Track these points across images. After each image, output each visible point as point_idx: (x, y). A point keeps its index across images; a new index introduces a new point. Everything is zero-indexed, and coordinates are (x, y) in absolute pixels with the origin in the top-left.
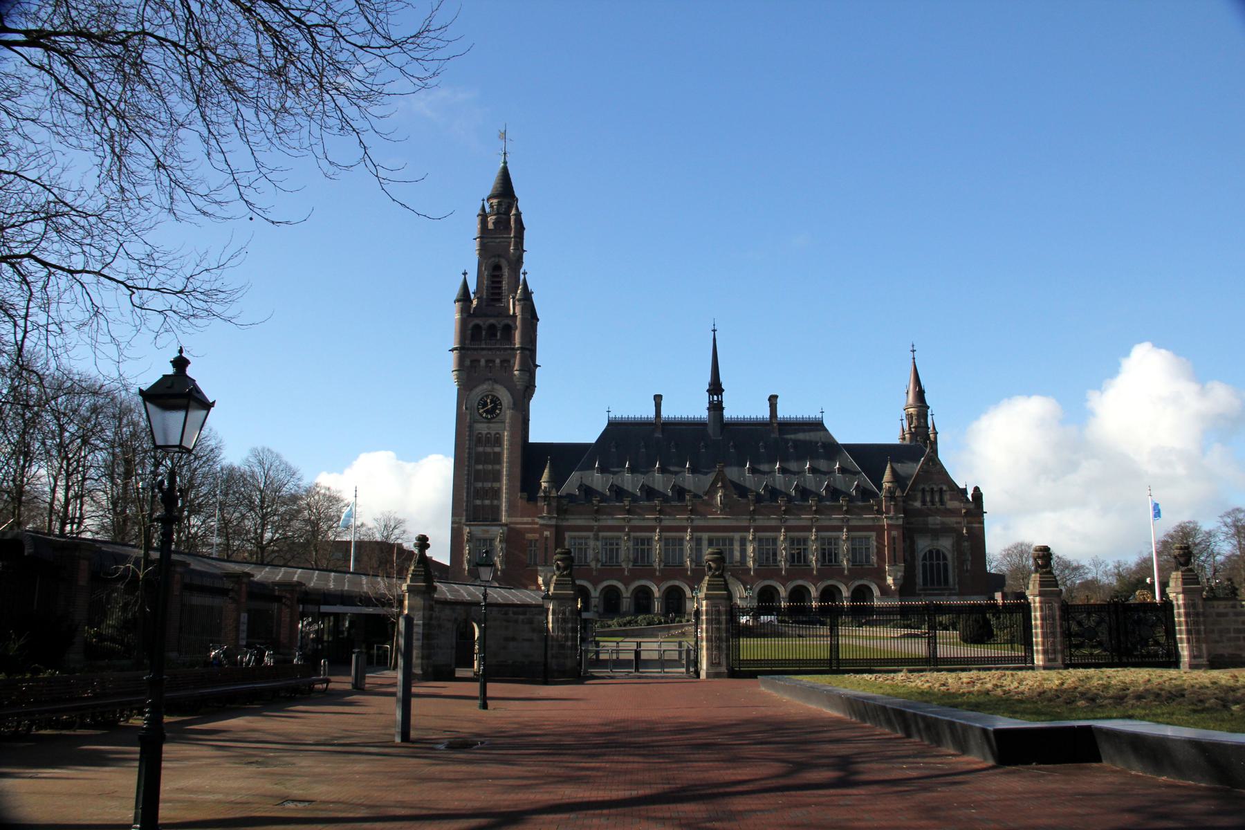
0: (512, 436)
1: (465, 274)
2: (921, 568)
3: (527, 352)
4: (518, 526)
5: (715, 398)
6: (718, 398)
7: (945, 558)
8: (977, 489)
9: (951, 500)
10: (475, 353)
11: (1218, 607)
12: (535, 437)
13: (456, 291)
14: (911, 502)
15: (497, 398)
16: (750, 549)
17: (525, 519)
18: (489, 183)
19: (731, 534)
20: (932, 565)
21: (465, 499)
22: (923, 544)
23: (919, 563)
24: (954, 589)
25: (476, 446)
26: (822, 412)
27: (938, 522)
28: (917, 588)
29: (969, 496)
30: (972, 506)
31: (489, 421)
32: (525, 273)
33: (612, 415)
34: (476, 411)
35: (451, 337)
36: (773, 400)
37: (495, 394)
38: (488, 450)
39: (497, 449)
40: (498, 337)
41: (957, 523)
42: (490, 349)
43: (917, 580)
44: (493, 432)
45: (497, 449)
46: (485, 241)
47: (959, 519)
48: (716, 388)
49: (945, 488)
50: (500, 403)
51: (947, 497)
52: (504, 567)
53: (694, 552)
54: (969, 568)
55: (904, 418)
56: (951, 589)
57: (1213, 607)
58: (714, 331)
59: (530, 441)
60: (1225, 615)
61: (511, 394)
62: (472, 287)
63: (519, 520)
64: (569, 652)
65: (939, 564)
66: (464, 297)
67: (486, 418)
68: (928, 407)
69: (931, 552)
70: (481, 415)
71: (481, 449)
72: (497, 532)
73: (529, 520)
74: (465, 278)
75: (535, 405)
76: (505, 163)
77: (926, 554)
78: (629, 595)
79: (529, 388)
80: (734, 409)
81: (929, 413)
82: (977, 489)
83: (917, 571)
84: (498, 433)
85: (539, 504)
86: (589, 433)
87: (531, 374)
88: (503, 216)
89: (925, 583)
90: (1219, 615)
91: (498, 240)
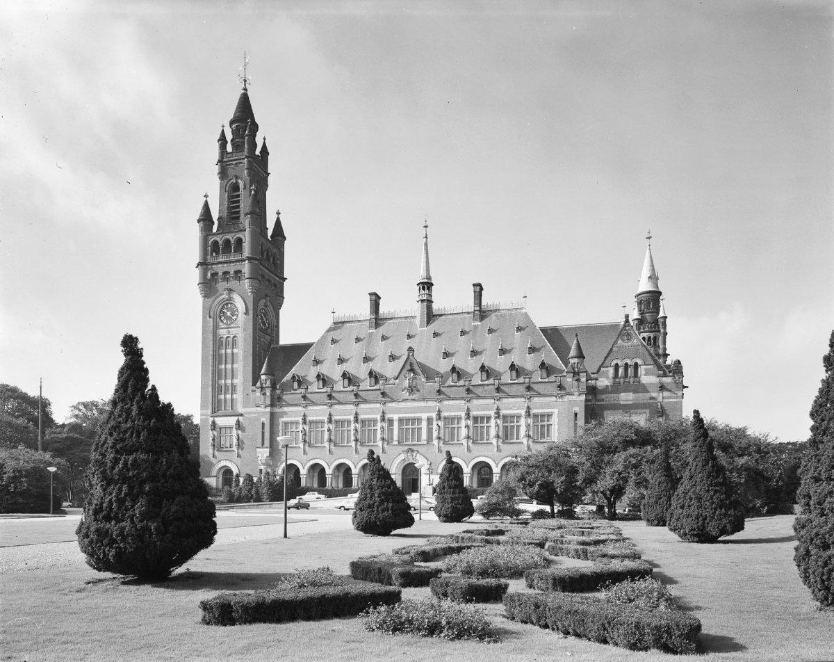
0: (245, 340)
1: (206, 196)
9: (646, 374)
13: (198, 212)
16: (435, 427)
18: (230, 111)
27: (631, 398)
39: (235, 351)
42: (227, 263)
49: (639, 362)
51: (642, 370)
53: (386, 432)
66: (206, 217)
70: (222, 321)
72: (232, 421)
76: (245, 89)
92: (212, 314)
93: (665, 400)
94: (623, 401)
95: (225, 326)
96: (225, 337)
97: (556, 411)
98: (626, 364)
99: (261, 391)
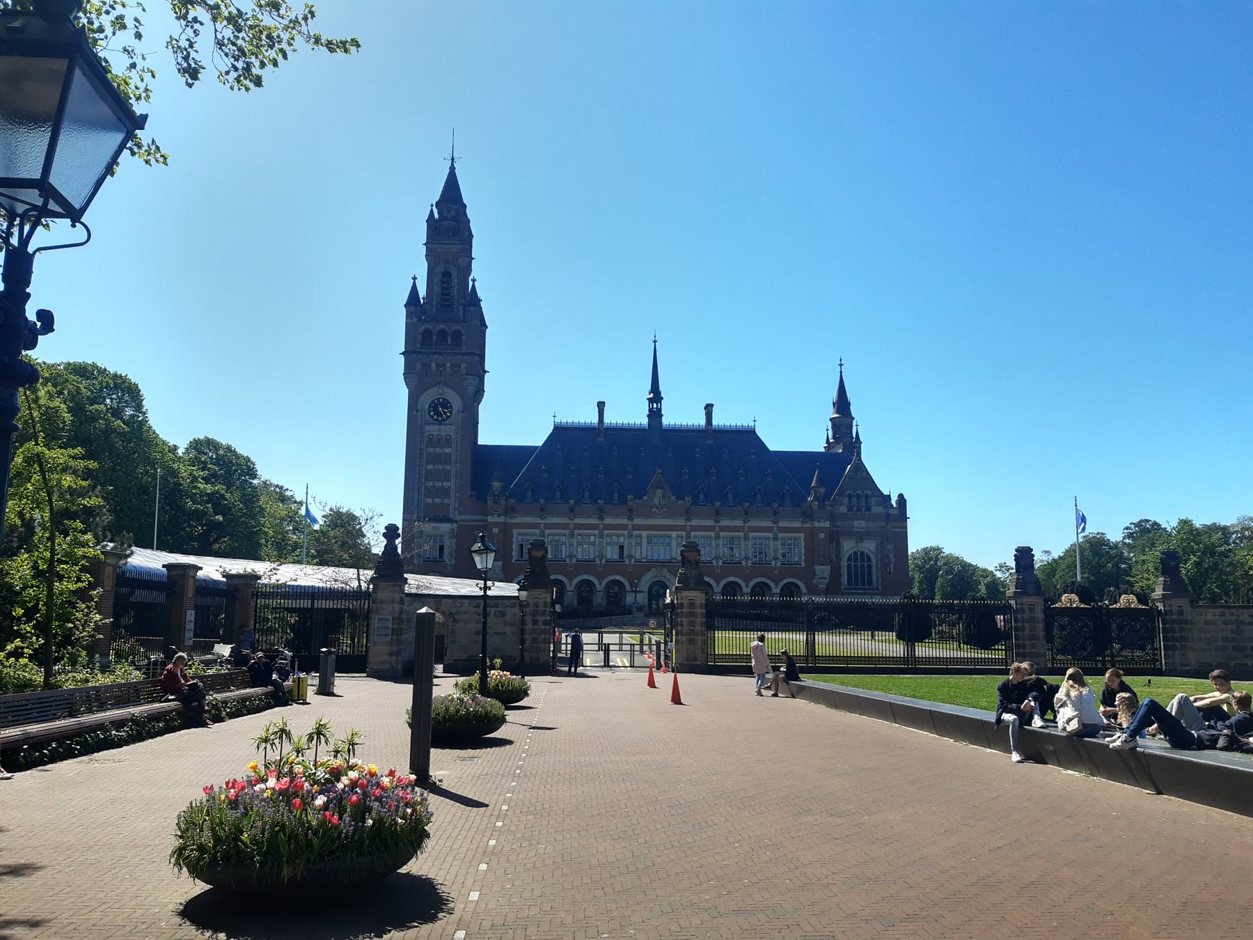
1: (415, 278)
2: (846, 568)
3: (476, 357)
4: (467, 523)
5: (655, 405)
6: (657, 406)
7: (869, 559)
8: (901, 496)
9: (876, 505)
10: (426, 356)
11: (1206, 615)
12: (486, 437)
14: (837, 507)
15: (448, 401)
17: (474, 517)
19: (669, 533)
20: (856, 566)
21: (416, 497)
22: (848, 546)
23: (844, 564)
24: (877, 589)
25: (427, 447)
26: (755, 421)
27: (863, 525)
28: (842, 587)
29: (894, 502)
30: (896, 512)
31: (440, 423)
32: (474, 280)
33: (558, 420)
34: (427, 415)
35: (399, 342)
36: (709, 408)
37: (445, 397)
38: (439, 450)
39: (448, 450)
40: (449, 342)
41: (882, 527)
42: (440, 354)
43: (842, 580)
44: (444, 434)
45: (448, 450)
46: (435, 246)
47: (883, 524)
48: (656, 396)
49: (869, 493)
50: (451, 406)
52: (453, 562)
54: (892, 570)
55: (830, 428)
56: (873, 589)
57: (1201, 615)
58: (655, 342)
59: (479, 443)
60: (1214, 623)
61: (461, 398)
62: (422, 292)
63: (469, 517)
64: (543, 645)
65: (863, 565)
67: (436, 420)
68: (854, 419)
69: (855, 553)
70: (432, 417)
71: (431, 450)
72: (446, 527)
73: (480, 517)
74: (414, 283)
75: (484, 409)
76: (452, 169)
77: (851, 555)
78: (572, 589)
79: (479, 392)
80: (670, 418)
81: (854, 423)
82: (901, 496)
83: (842, 571)
84: (448, 435)
85: (488, 502)
86: (535, 435)
87: (480, 379)
88: (453, 223)
89: (849, 582)
90: (1207, 623)
91: (445, 246)
92: (419, 408)
93: (893, 530)
94: (857, 528)
95: (436, 422)
96: (435, 434)
97: (802, 535)
98: (858, 496)
99: (494, 499)
